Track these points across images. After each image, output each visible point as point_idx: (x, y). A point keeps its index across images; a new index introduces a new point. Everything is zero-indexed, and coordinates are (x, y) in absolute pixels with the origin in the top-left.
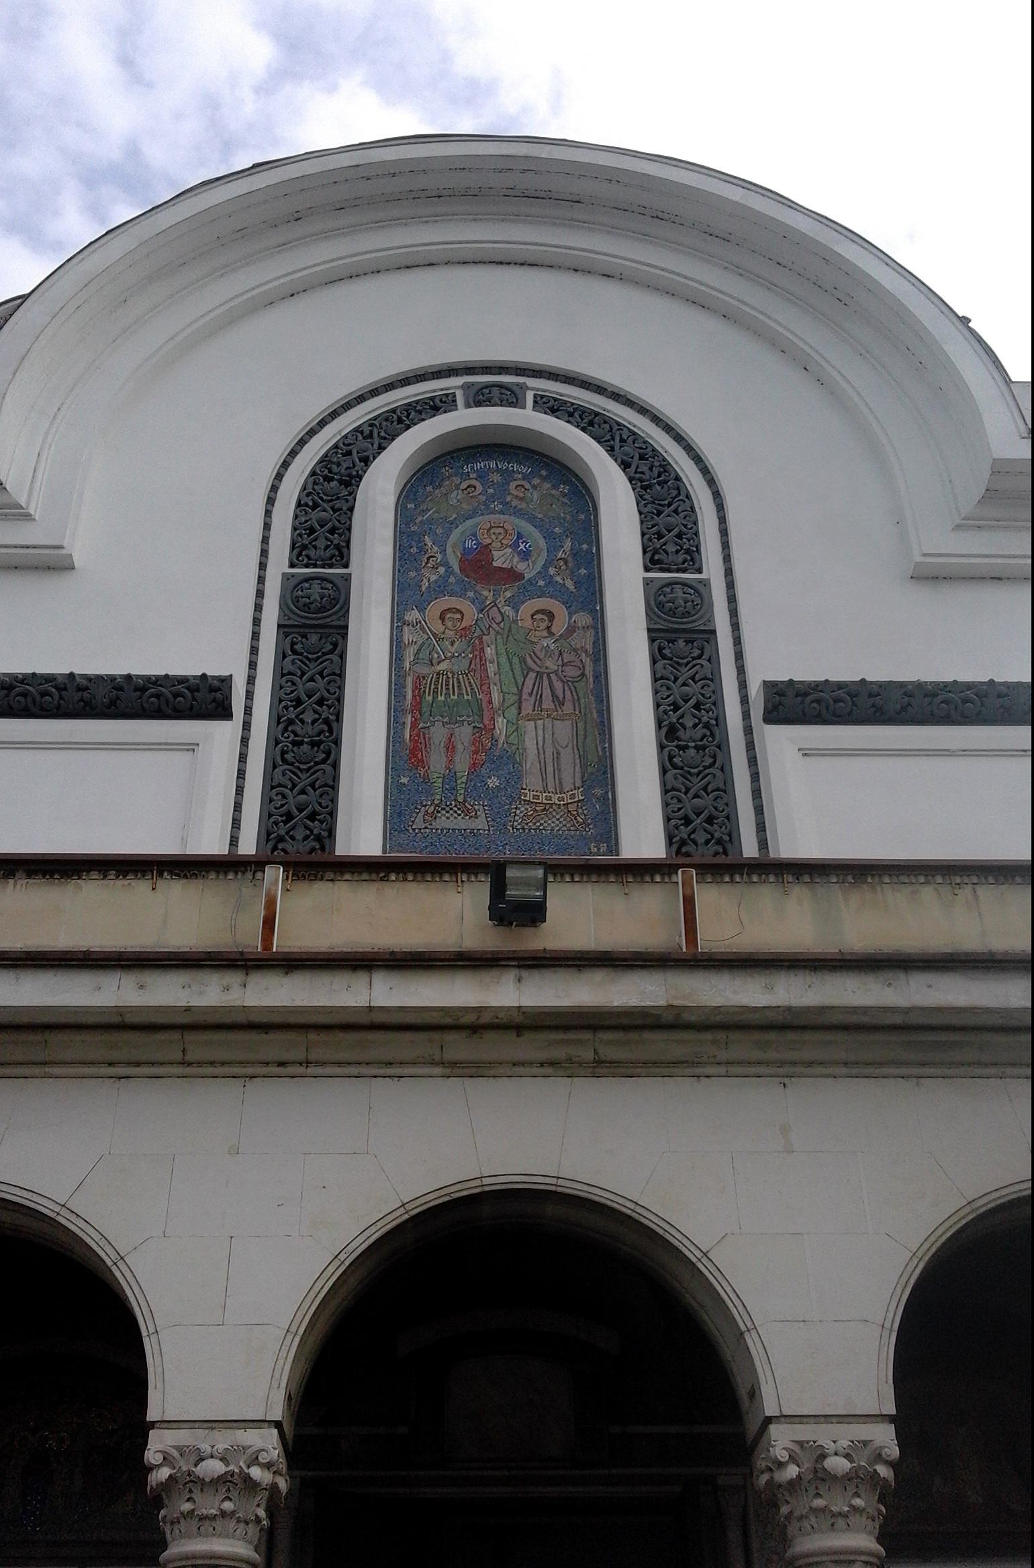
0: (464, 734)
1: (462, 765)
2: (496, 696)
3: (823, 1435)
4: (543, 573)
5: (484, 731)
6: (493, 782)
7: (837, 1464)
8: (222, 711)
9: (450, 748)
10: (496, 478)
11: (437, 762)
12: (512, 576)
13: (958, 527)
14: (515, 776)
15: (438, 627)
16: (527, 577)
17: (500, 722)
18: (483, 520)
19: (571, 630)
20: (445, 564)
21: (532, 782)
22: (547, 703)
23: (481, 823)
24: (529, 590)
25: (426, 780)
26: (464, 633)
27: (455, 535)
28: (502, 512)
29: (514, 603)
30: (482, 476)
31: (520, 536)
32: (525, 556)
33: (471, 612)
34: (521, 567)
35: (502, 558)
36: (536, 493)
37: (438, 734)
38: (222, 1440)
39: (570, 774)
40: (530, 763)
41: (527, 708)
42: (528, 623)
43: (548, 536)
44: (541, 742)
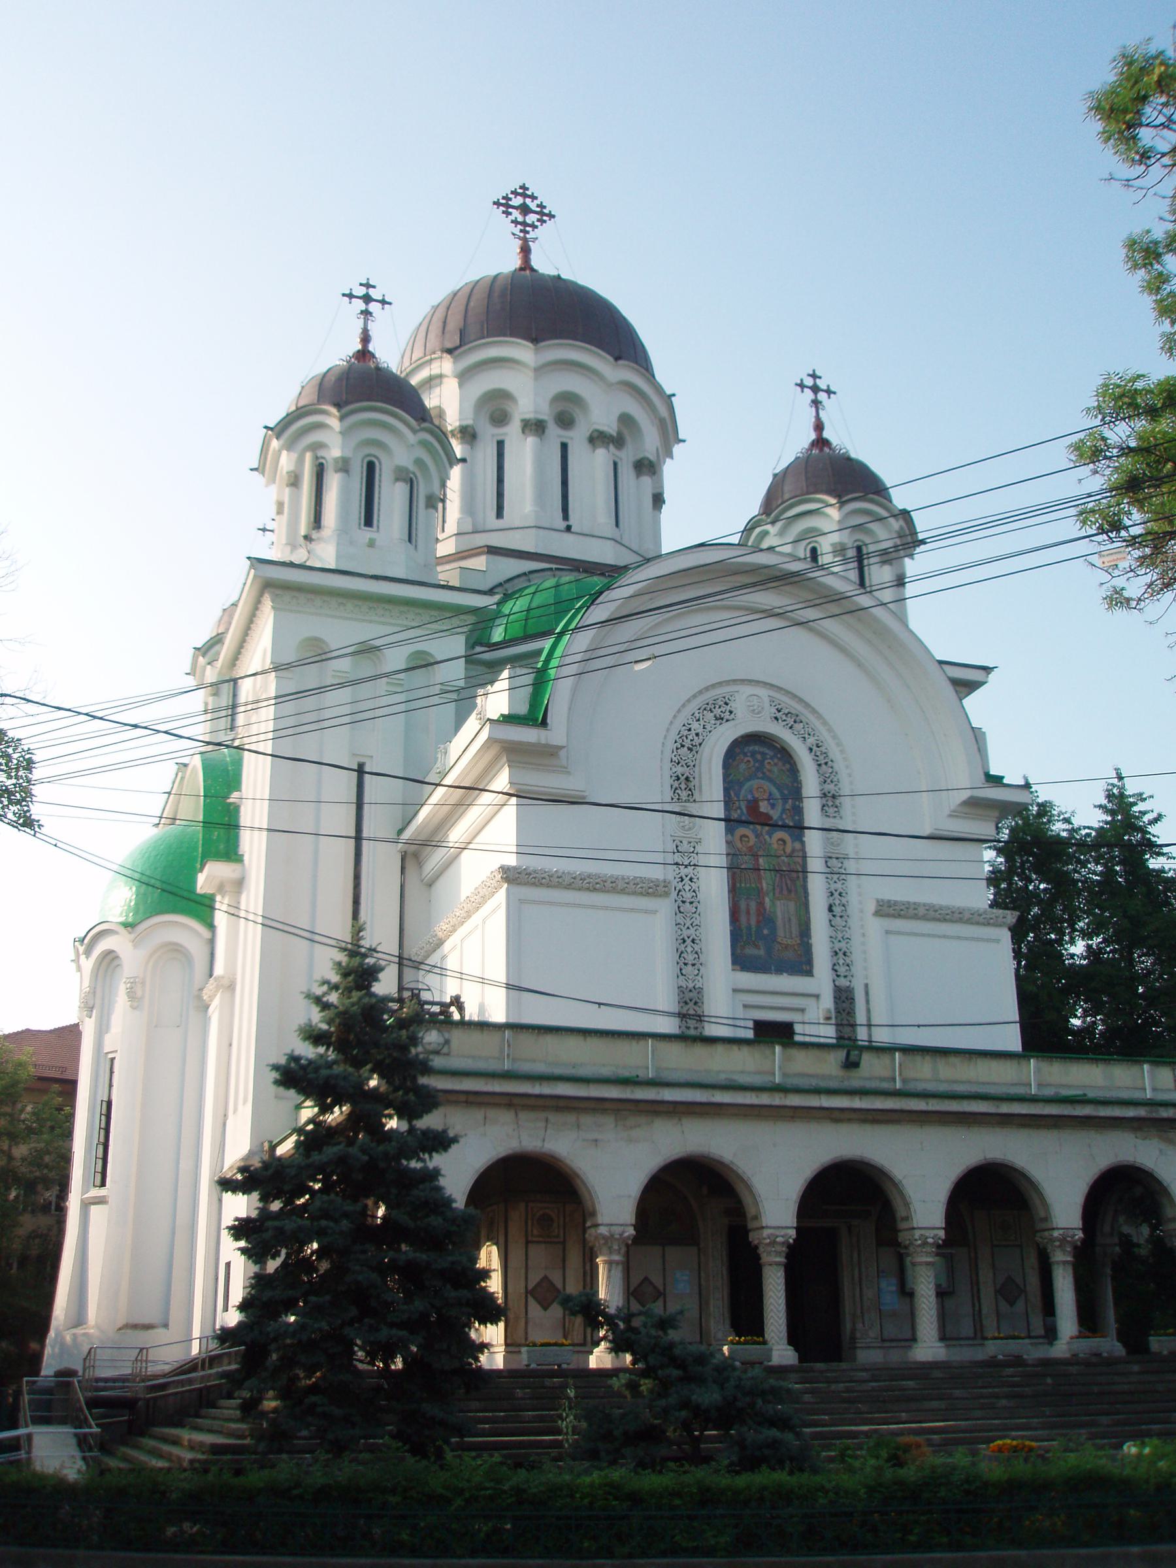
0: (753, 905)
1: (753, 922)
2: (764, 885)
3: (927, 1233)
4: (781, 818)
5: (761, 904)
6: (766, 932)
7: (930, 1240)
8: (666, 894)
9: (748, 913)
10: (759, 757)
11: (743, 919)
13: (950, 816)
14: (774, 929)
15: (739, 845)
17: (767, 900)
18: (754, 783)
20: (740, 808)
21: (780, 933)
22: (785, 892)
23: (762, 952)
25: (740, 928)
26: (750, 849)
28: (762, 778)
29: (770, 834)
30: (753, 754)
31: (770, 794)
32: (773, 806)
33: (753, 839)
34: (771, 812)
35: (764, 807)
36: (775, 768)
37: (743, 905)
38: (783, 1232)
39: (795, 930)
40: (779, 923)
41: (777, 891)
42: (775, 846)
44: (781, 909)
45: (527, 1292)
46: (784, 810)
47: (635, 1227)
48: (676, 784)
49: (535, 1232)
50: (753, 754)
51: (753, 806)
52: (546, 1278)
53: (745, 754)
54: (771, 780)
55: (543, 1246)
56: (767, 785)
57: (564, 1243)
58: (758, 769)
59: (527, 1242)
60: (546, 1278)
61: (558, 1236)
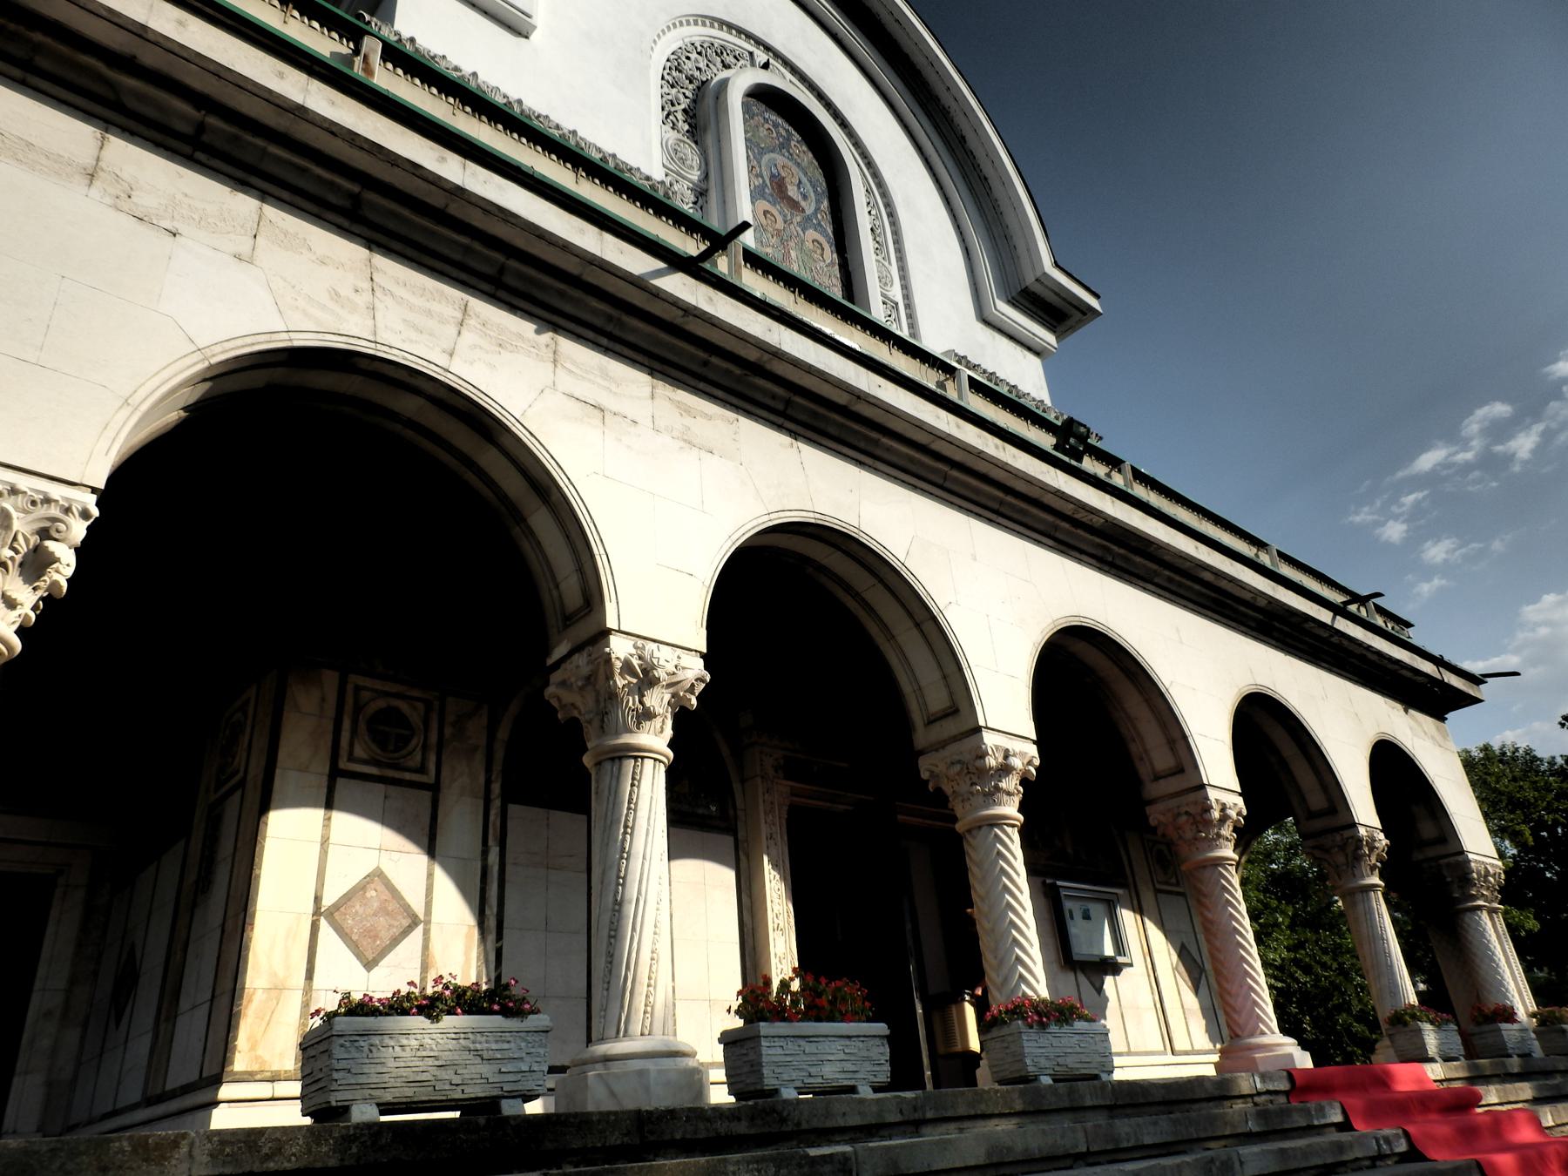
12: (794, 205)
16: (808, 212)
19: (832, 264)
24: (806, 223)
27: (766, 158)
30: (776, 125)
32: (805, 197)
33: (780, 225)
34: (803, 204)
35: (792, 192)
43: (815, 191)
45: (317, 912)
46: (817, 209)
47: (709, 659)
48: (668, 107)
49: (359, 752)
50: (776, 125)
51: (779, 185)
52: (378, 875)
53: (766, 121)
54: (798, 165)
55: (380, 788)
56: (795, 169)
57: (435, 789)
58: (782, 146)
59: (335, 774)
60: (378, 875)
61: (422, 770)
